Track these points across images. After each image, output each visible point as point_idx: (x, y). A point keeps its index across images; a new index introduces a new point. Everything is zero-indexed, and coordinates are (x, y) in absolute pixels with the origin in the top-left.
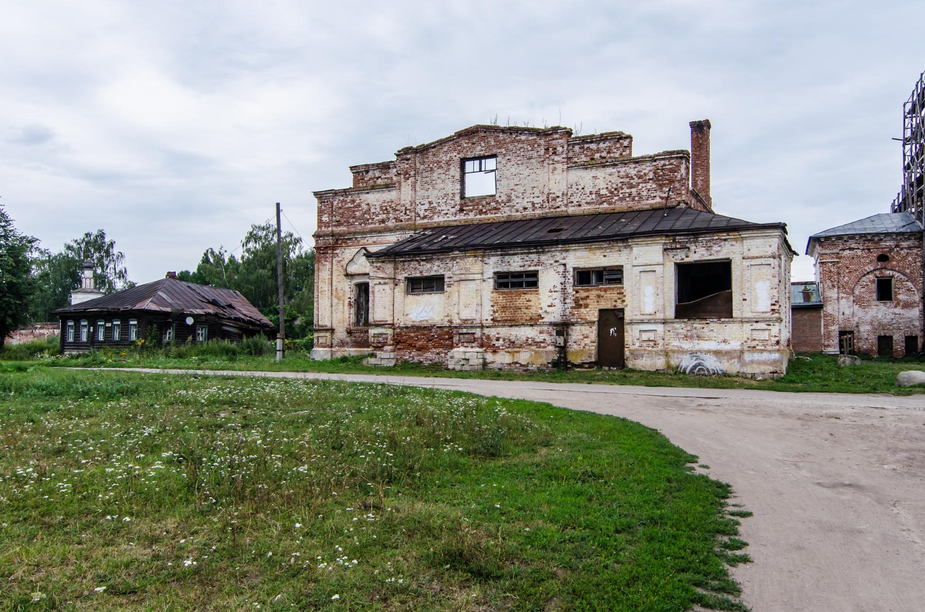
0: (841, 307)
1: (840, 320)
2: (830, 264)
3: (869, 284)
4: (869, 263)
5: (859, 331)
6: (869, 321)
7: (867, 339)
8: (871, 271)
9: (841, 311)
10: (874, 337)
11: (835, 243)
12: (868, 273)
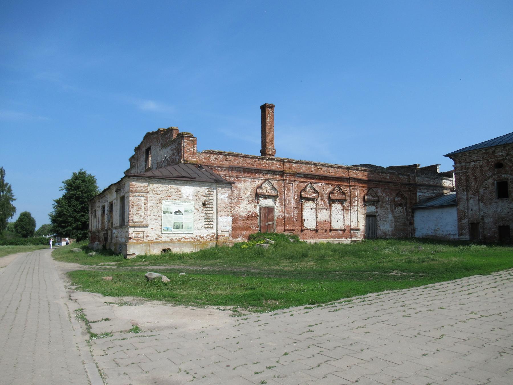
0: (470, 205)
2: (461, 174)
3: (490, 186)
5: (484, 223)
7: (490, 228)
9: (470, 208)
10: (495, 227)
11: (463, 158)
12: (489, 178)
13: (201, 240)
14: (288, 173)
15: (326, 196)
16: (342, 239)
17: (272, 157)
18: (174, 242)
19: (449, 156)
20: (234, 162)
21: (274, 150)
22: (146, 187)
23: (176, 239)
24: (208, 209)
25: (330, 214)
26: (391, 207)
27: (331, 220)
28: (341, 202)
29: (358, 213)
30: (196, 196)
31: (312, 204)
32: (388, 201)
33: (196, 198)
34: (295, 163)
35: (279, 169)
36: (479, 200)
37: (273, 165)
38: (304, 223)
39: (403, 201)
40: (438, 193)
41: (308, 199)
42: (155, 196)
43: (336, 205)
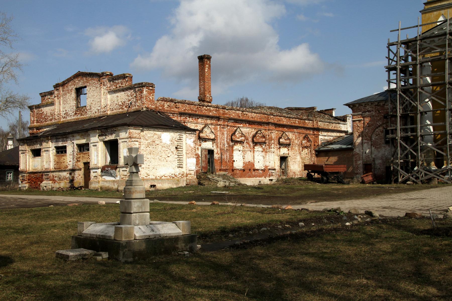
1: (364, 157)
2: (357, 122)
3: (380, 133)
4: (379, 120)
5: (375, 164)
6: (381, 157)
7: (379, 168)
8: (381, 125)
10: (383, 167)
11: (359, 108)
12: (379, 126)
13: (175, 178)
14: (222, 119)
15: (250, 139)
16: (262, 178)
17: (209, 104)
18: (157, 179)
19: (348, 105)
20: (183, 109)
21: (211, 98)
22: (139, 134)
23: (159, 177)
24: (180, 152)
25: (254, 156)
26: (299, 150)
27: (254, 161)
28: (261, 144)
29: (275, 154)
30: (171, 141)
31: (240, 146)
32: (297, 144)
33: (172, 143)
34: (227, 110)
35: (216, 115)
36: (371, 145)
37: (210, 111)
38: (234, 163)
39: (308, 144)
40: (335, 136)
41: (237, 142)
42: (145, 141)
43: (258, 147)
